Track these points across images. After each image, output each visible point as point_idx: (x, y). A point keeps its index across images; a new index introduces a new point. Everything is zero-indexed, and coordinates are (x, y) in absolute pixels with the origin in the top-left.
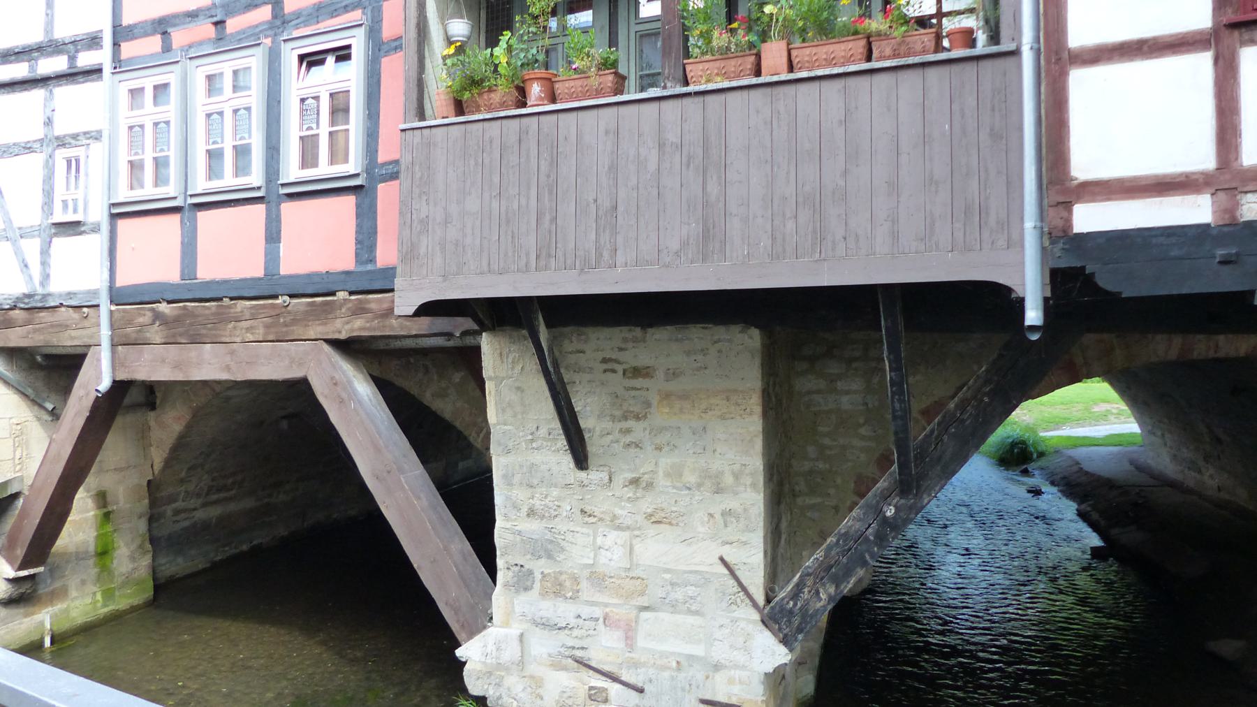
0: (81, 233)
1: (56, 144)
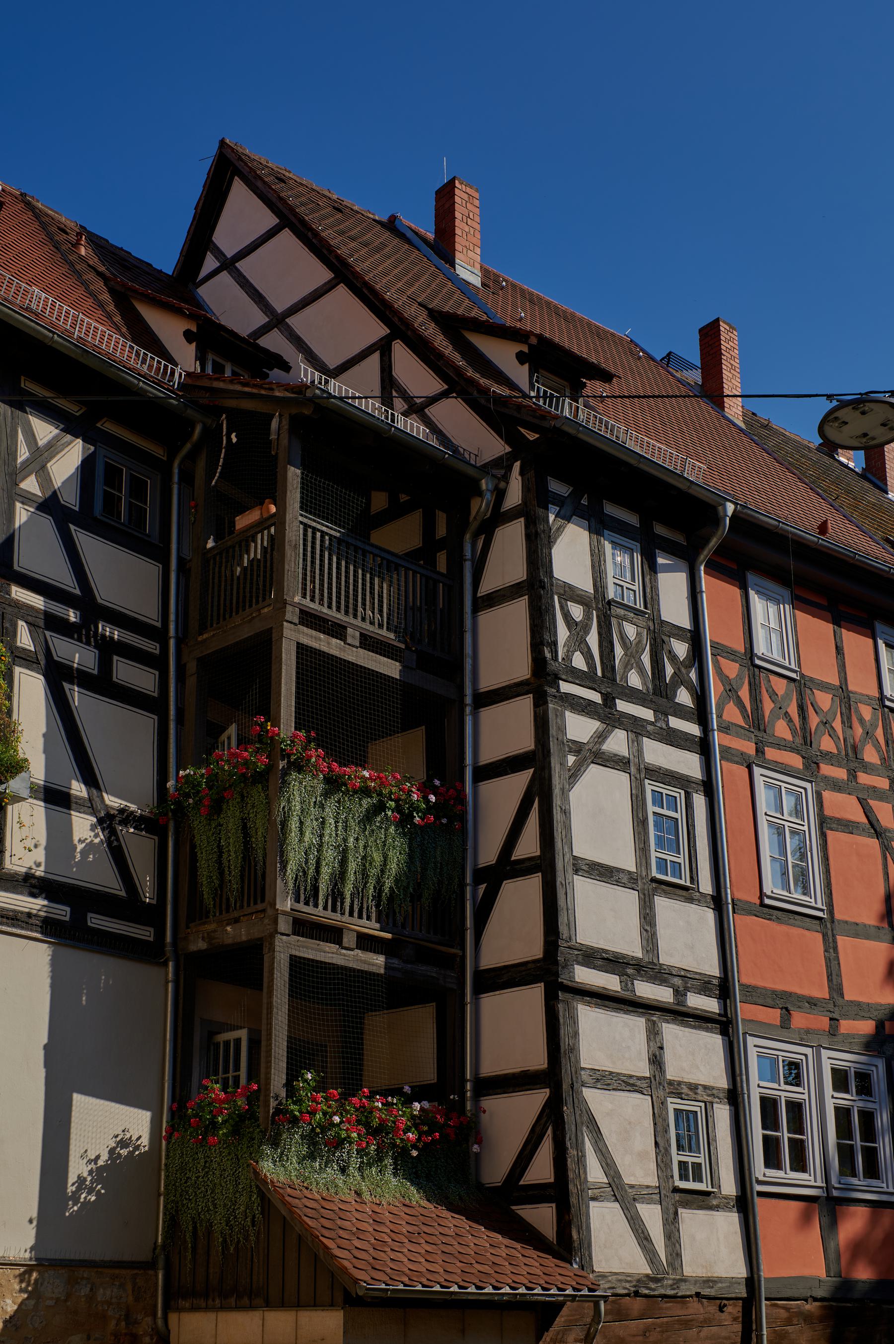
0: (711, 1208)
1: (667, 1091)
